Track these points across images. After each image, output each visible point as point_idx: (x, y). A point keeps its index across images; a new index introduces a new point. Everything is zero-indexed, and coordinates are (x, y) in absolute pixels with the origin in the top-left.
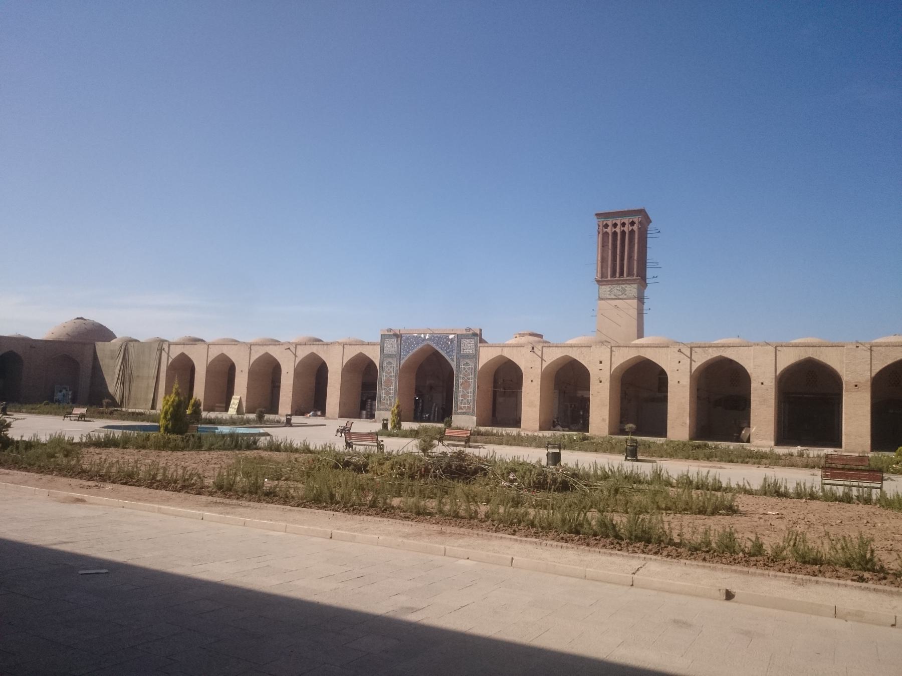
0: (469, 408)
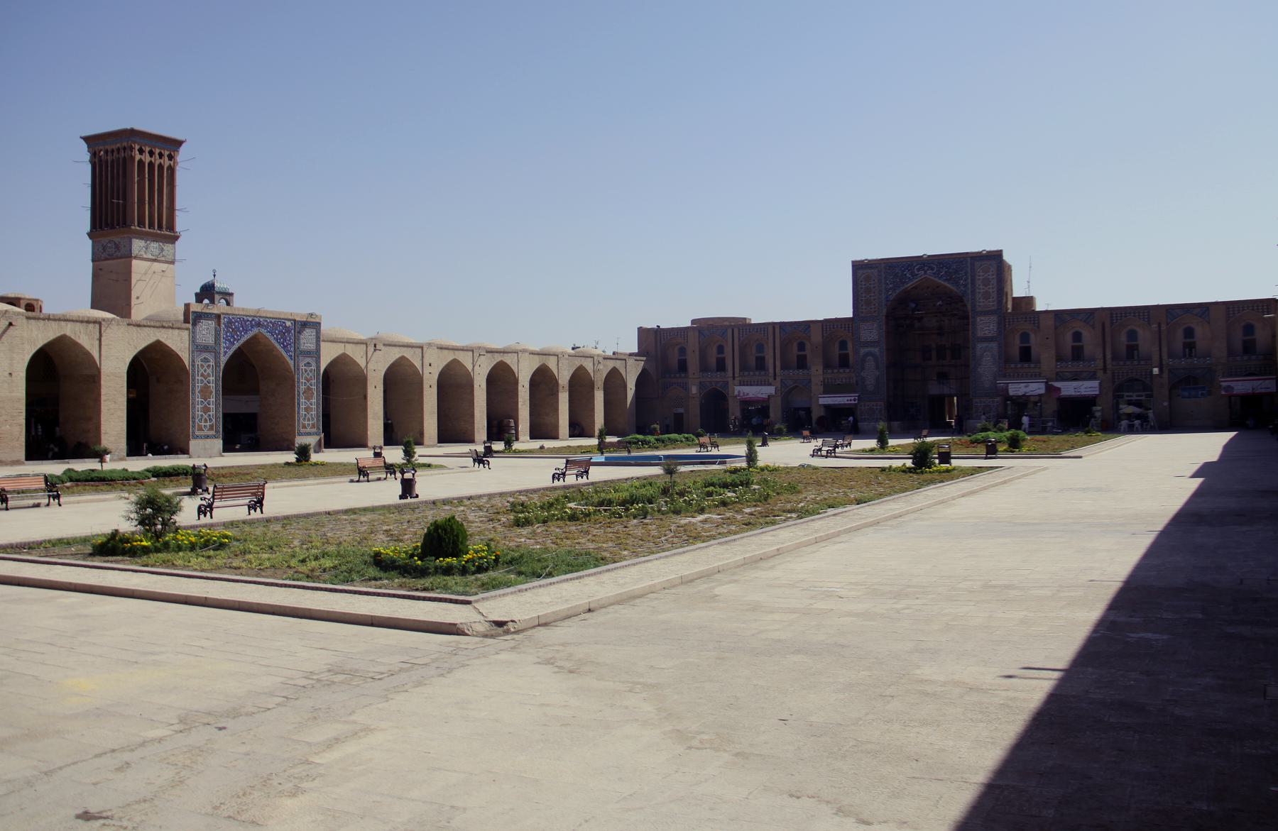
0: (313, 426)
